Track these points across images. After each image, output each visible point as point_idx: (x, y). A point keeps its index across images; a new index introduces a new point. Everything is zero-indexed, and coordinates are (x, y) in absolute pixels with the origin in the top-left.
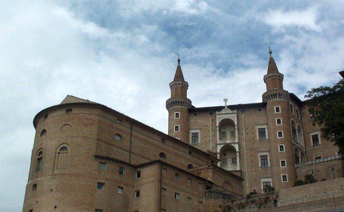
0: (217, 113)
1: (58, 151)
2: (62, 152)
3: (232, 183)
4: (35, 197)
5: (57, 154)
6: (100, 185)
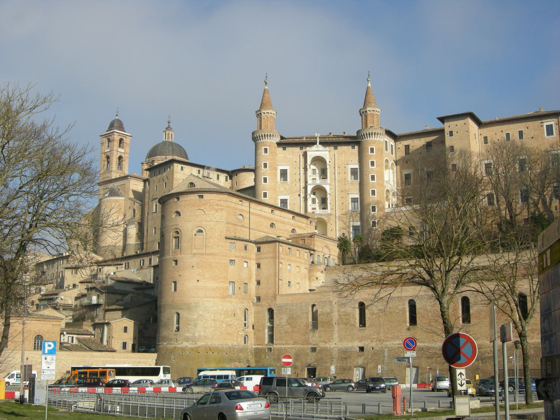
0: (308, 149)
1: (194, 232)
2: (198, 234)
3: (330, 247)
4: (178, 271)
5: (194, 236)
6: (231, 261)
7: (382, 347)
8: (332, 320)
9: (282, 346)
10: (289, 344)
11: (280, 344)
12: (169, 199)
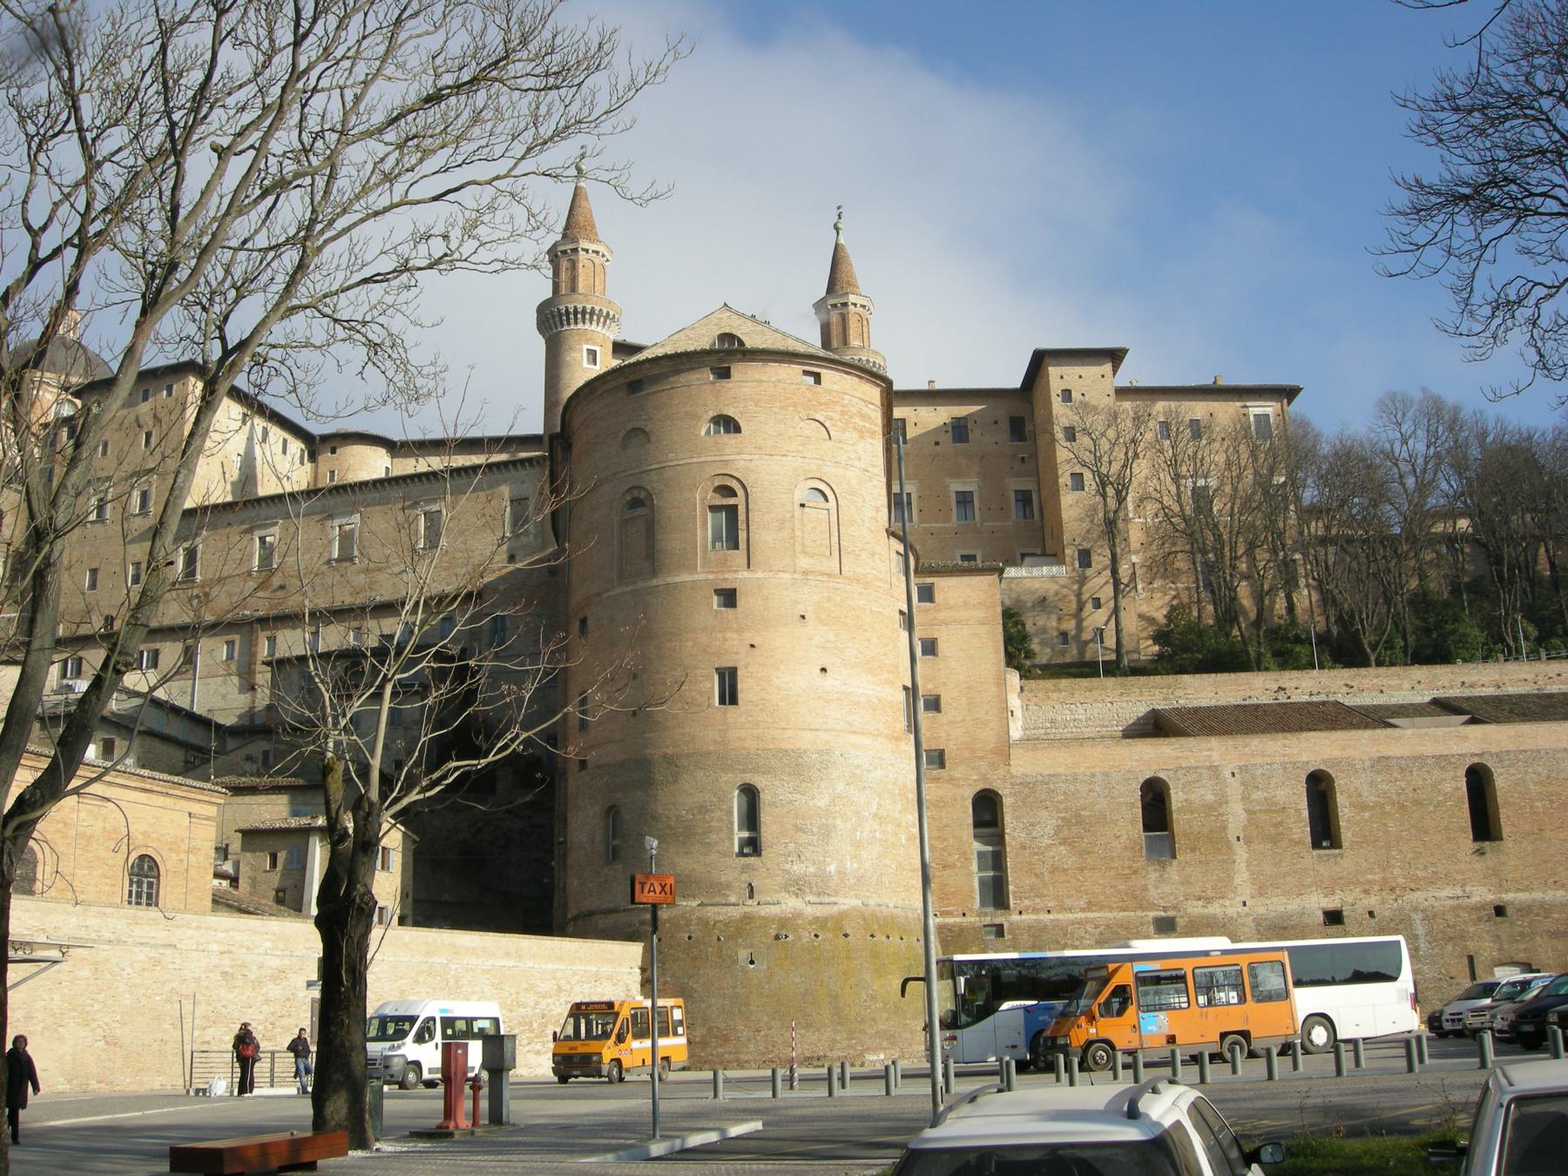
4: (739, 631)
5: (797, 507)
7: (1401, 909)
8: (1225, 828)
9: (1045, 917)
10: (1070, 910)
11: (1035, 910)
12: (678, 372)
